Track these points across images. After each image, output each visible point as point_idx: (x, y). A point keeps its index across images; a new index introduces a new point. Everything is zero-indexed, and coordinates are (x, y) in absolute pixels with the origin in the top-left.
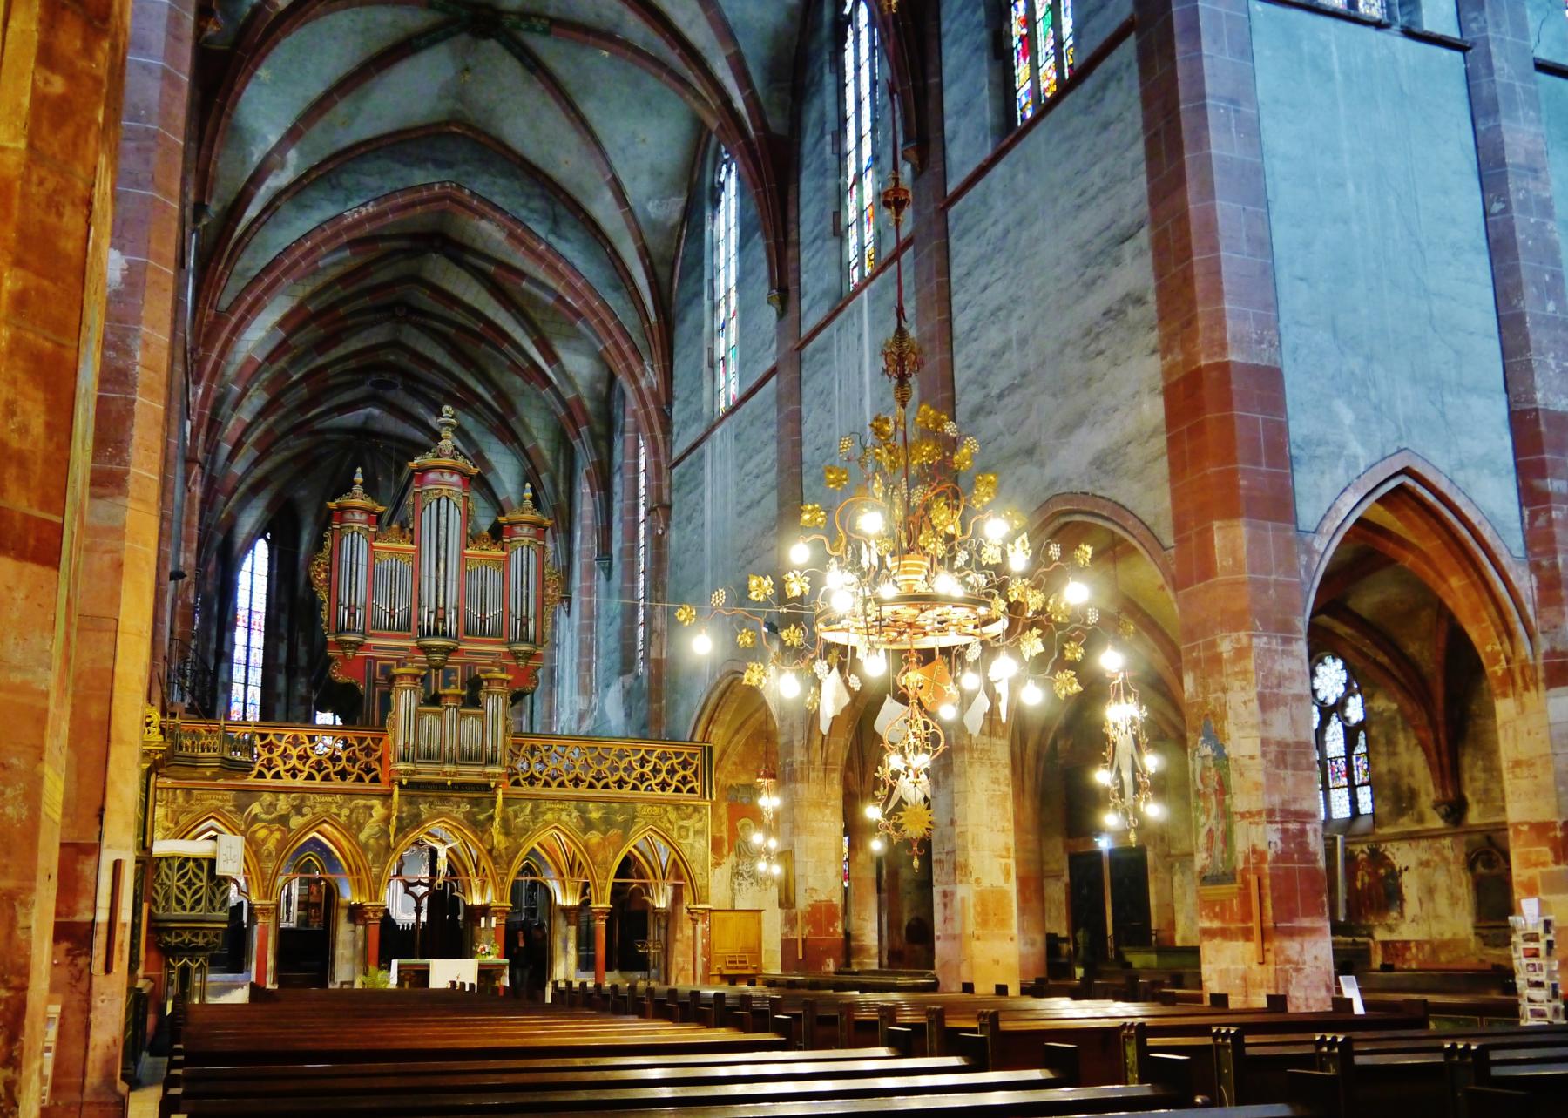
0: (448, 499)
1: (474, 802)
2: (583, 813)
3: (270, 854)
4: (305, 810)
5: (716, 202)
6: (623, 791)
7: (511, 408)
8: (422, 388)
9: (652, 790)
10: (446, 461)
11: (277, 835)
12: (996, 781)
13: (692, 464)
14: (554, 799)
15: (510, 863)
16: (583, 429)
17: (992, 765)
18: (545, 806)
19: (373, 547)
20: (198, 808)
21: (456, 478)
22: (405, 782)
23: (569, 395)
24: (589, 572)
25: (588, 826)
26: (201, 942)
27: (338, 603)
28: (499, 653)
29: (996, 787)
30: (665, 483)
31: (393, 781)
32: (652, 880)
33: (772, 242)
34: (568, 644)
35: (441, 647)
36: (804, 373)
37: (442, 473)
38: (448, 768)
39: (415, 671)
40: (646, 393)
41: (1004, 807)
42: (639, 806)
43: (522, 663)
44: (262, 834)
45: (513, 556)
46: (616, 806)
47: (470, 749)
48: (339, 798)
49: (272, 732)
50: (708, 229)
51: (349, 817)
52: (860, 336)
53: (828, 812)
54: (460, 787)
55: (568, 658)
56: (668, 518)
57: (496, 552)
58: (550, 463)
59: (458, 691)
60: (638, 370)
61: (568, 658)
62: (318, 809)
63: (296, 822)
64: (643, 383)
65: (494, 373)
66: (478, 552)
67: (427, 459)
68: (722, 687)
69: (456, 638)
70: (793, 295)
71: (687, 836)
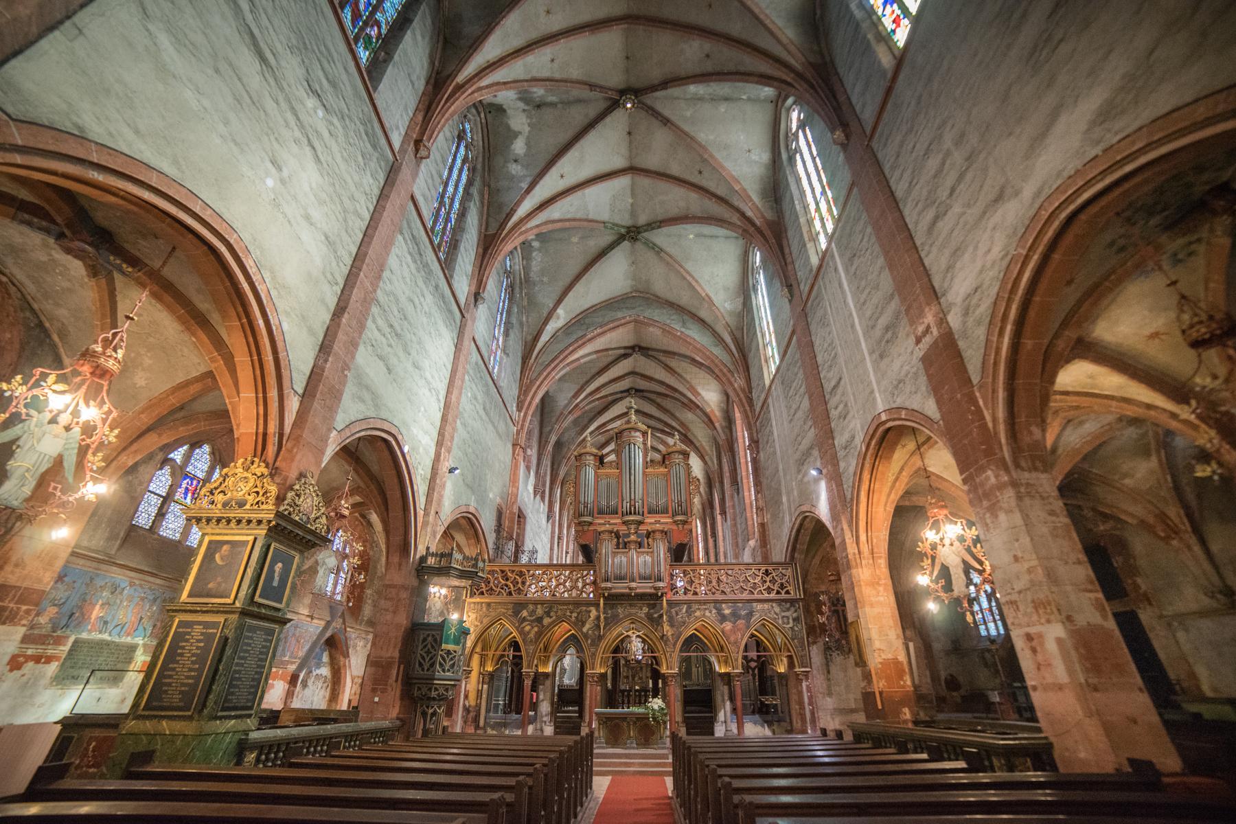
1: (652, 606)
2: (719, 611)
3: (531, 641)
4: (552, 614)
5: (755, 290)
7: (688, 429)
11: (536, 629)
12: (1052, 513)
14: (700, 602)
15: (675, 645)
17: (1043, 498)
18: (695, 607)
20: (493, 614)
23: (708, 410)
25: (723, 618)
26: (434, 694)
27: (579, 502)
28: (667, 523)
29: (1054, 518)
32: (773, 653)
33: (778, 267)
36: (809, 319)
38: (634, 585)
40: (738, 389)
41: (1071, 538)
42: (755, 604)
44: (528, 628)
46: (740, 605)
48: (570, 607)
50: (754, 303)
51: (576, 618)
52: (836, 269)
53: (881, 589)
54: (641, 597)
57: (662, 470)
60: (732, 380)
62: (559, 613)
63: (546, 621)
64: (736, 385)
65: (678, 414)
68: (796, 526)
70: (795, 286)
71: (788, 623)
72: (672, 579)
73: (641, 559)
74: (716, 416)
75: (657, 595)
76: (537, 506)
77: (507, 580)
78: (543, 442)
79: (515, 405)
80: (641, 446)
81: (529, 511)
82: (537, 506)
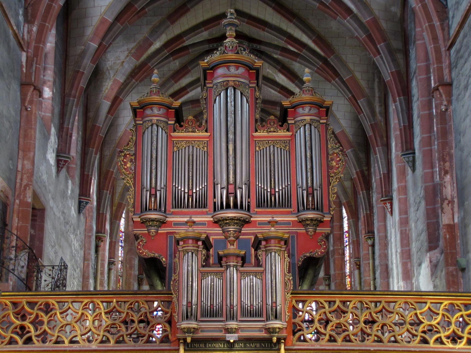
0: (235, 89)
6: (412, 344)
8: (263, 48)
9: (442, 343)
10: (231, 56)
13: (465, 36)
16: (381, 46)
19: (172, 137)
21: (241, 70)
22: (189, 340)
24: (403, 174)
28: (287, 223)
30: (445, 64)
31: (179, 339)
34: (393, 240)
35: (232, 219)
37: (228, 68)
38: (233, 324)
39: (198, 235)
43: (311, 229)
45: (298, 135)
47: (252, 305)
49: (70, 300)
55: (394, 251)
56: (449, 95)
57: (282, 133)
58: (367, 91)
59: (237, 252)
61: (394, 251)
66: (265, 134)
67: (216, 57)
69: (249, 210)
72: (295, 316)
73: (246, 281)
74: (379, 28)
75: (269, 340)
76: (62, 187)
77: (24, 318)
78: (70, 73)
79: (21, 12)
80: (248, 92)
81: (50, 196)
82: (62, 187)
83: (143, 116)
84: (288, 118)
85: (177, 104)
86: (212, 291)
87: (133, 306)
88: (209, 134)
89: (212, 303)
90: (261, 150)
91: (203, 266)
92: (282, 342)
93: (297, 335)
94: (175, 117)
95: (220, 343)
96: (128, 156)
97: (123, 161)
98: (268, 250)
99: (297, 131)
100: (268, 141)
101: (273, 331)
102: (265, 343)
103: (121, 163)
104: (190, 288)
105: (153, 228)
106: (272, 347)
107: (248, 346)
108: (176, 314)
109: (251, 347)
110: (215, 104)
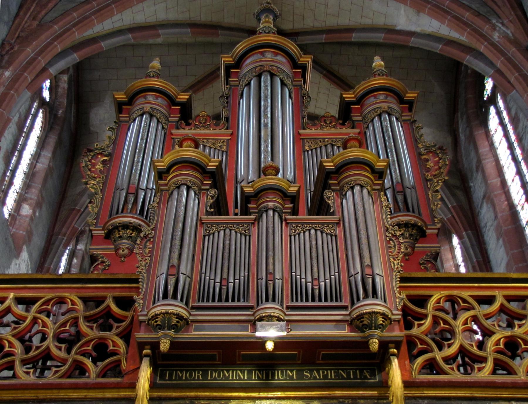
37: (262, 54)
45: (370, 133)
83: (129, 112)
84: (352, 115)
85: (183, 97)
86: (226, 254)
87: (49, 307)
88: (230, 132)
89: (225, 276)
90: (312, 150)
91: (208, 213)
92: (394, 355)
93: (420, 360)
94: (180, 113)
95: (241, 371)
96: (99, 156)
97: (90, 161)
98: (347, 183)
99: (368, 126)
100: (324, 139)
101: (371, 321)
102: (347, 369)
103: (86, 164)
104: (177, 242)
105: (124, 241)
106: (366, 378)
107: (307, 376)
108: (141, 296)
109: (315, 378)
110: (241, 100)
